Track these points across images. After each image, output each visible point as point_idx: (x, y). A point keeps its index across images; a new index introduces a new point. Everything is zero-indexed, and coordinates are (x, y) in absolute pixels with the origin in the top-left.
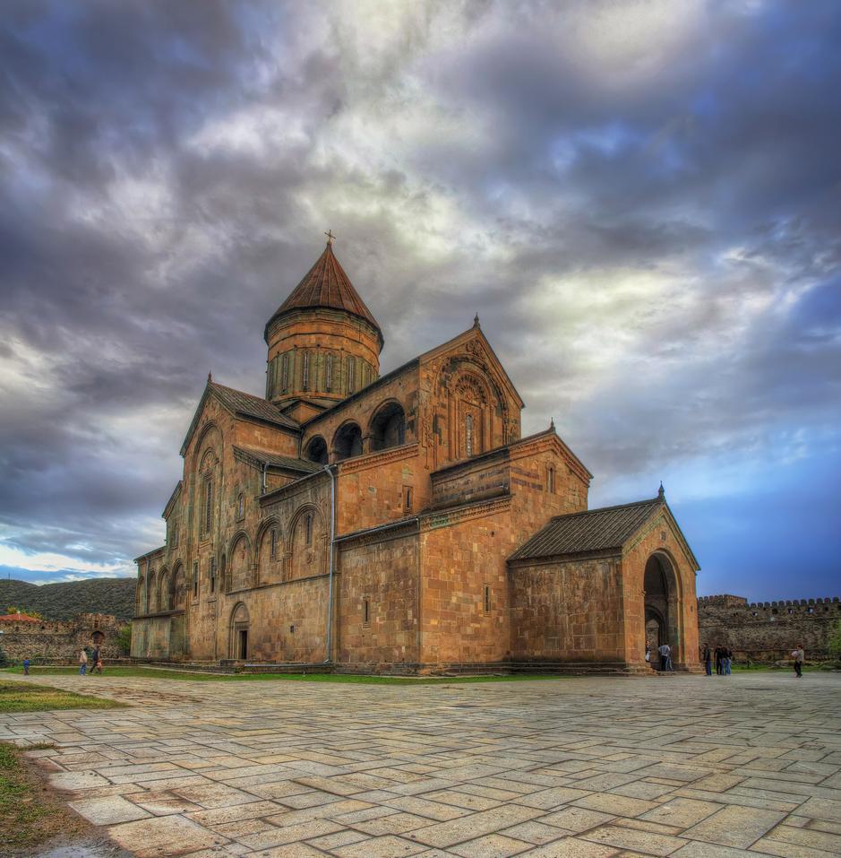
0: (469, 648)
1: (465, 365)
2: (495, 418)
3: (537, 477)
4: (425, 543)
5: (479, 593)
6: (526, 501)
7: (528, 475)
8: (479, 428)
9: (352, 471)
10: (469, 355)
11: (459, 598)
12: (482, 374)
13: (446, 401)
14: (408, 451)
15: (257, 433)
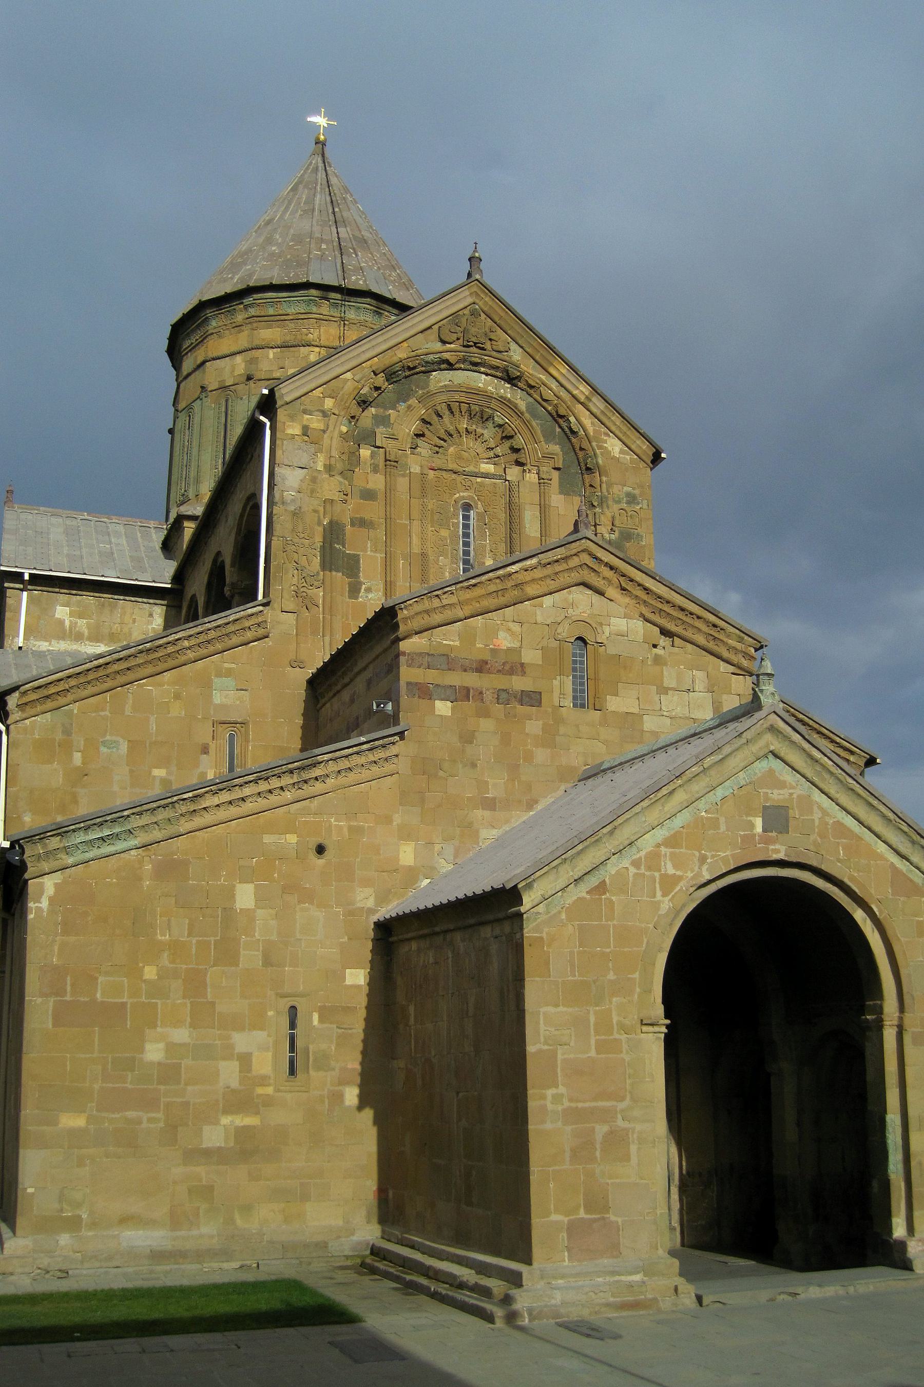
0: (211, 1188)
1: (440, 379)
2: (556, 500)
3: (518, 668)
4: (44, 904)
5: (258, 1022)
6: (468, 738)
7: (481, 667)
8: (502, 530)
9: (50, 704)
10: (452, 351)
11: (171, 1048)
12: (505, 390)
13: (377, 482)
14: (231, 628)
15: (62, 612)
